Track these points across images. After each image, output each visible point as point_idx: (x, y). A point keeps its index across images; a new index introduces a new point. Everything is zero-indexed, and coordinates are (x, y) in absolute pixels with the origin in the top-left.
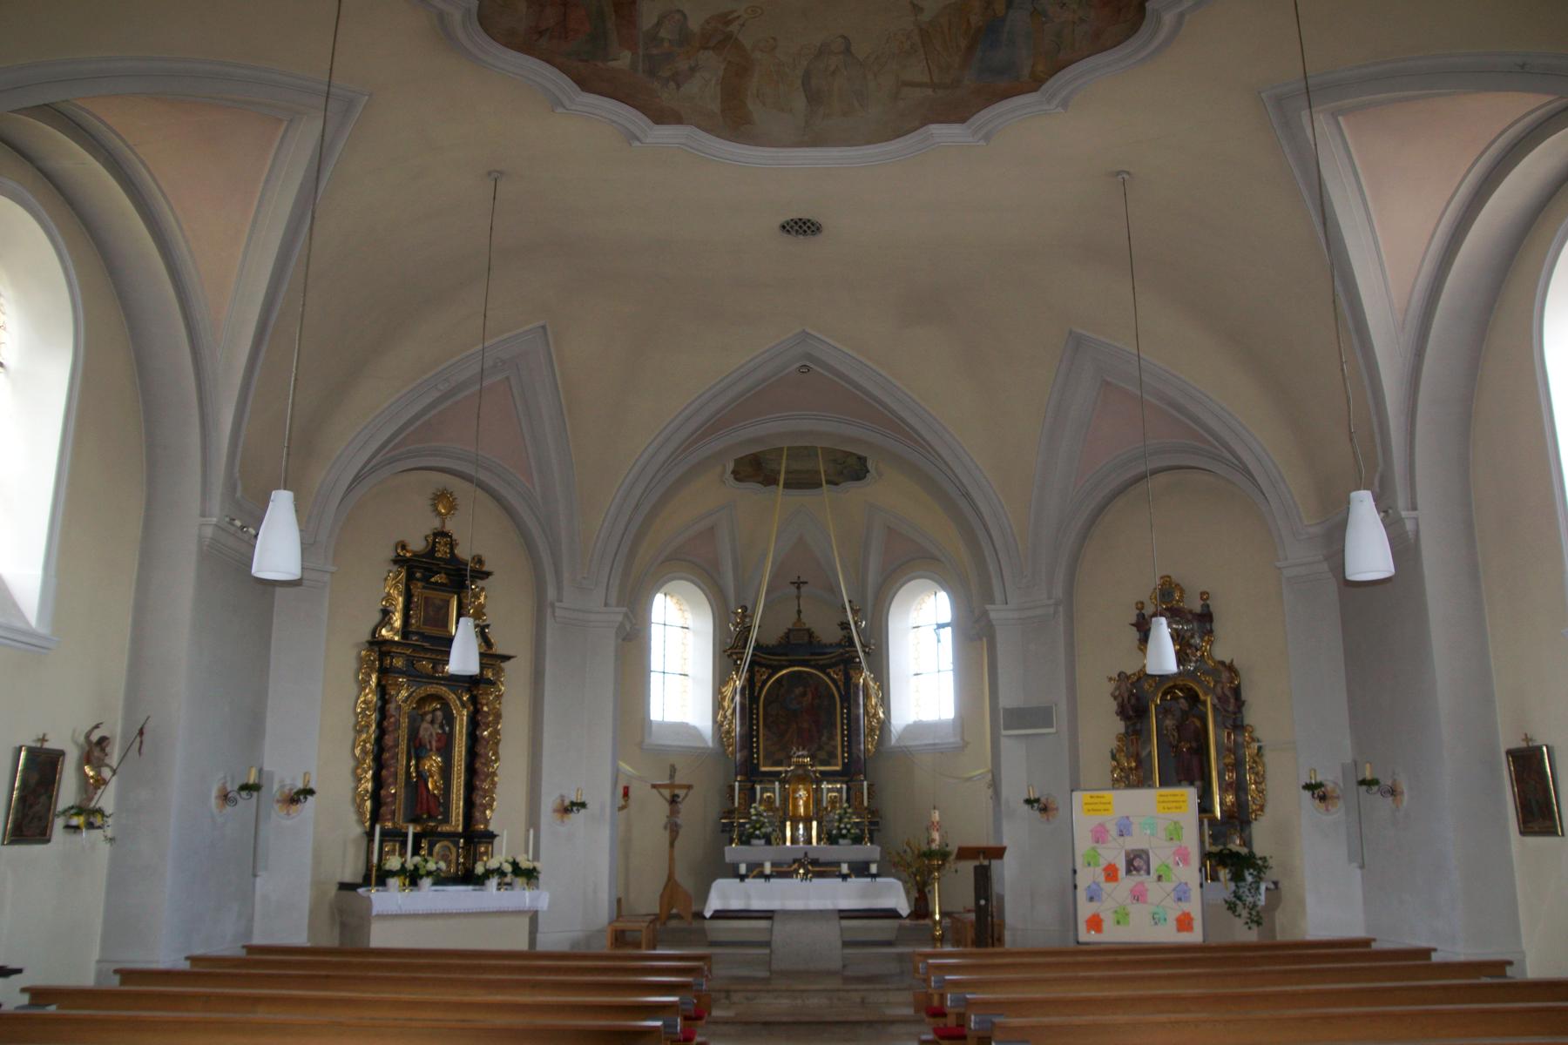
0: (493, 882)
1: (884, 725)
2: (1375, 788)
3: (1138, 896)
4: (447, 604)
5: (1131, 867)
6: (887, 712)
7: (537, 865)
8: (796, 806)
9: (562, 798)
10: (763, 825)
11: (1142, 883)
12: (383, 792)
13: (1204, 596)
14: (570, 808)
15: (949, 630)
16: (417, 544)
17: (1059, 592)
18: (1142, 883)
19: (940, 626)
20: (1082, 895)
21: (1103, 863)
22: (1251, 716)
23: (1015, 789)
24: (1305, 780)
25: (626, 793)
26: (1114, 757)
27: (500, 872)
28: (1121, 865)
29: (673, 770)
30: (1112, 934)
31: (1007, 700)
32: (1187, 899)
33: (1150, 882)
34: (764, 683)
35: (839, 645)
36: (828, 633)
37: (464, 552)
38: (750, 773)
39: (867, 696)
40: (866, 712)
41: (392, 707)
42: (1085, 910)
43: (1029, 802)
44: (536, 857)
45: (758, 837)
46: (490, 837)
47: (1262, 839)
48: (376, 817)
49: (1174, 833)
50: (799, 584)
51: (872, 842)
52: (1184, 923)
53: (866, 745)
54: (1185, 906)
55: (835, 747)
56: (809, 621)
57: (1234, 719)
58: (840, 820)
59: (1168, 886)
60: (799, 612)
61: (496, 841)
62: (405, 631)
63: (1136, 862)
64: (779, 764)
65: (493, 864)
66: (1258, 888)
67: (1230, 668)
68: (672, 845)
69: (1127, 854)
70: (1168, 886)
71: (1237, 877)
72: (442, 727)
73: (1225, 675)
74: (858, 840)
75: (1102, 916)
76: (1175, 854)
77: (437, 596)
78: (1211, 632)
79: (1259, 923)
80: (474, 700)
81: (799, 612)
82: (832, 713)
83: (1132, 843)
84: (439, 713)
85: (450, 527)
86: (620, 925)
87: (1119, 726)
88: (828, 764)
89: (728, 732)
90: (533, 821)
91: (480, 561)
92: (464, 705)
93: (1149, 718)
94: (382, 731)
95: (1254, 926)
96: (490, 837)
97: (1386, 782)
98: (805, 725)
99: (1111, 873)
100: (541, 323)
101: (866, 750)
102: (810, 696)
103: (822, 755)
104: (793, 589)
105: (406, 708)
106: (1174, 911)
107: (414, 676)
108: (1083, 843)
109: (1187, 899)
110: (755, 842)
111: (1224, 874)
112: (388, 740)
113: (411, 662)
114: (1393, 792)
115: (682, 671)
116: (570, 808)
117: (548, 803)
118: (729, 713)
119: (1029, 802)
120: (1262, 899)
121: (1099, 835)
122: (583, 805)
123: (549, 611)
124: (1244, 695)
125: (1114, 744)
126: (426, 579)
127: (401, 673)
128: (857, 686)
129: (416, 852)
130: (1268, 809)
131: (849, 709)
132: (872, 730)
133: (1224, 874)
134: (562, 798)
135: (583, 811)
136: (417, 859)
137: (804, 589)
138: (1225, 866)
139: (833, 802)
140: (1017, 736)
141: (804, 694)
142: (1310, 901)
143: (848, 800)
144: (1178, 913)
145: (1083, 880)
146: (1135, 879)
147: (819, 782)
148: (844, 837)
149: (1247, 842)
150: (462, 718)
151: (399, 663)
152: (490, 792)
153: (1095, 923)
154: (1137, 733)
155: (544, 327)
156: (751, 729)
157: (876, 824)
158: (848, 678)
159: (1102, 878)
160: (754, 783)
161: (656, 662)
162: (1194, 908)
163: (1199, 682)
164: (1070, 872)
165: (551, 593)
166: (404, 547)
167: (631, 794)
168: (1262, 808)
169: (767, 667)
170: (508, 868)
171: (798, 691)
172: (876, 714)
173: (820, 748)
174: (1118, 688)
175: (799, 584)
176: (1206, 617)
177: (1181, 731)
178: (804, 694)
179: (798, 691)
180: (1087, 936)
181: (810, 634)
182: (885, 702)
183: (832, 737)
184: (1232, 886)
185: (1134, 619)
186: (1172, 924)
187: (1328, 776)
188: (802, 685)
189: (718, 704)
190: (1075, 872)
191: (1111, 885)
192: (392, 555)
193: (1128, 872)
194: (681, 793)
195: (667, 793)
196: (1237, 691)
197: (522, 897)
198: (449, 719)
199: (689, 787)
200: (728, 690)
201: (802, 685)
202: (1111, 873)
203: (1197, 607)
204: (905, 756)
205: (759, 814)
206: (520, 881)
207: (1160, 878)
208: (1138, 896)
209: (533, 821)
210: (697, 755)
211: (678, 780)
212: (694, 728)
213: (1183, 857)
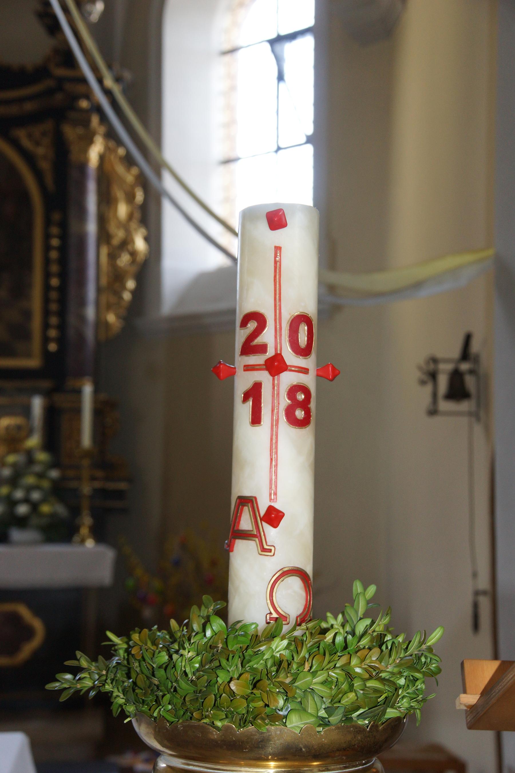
1: (148, 270)
6: (155, 240)
15: (308, 42)
35: (41, 72)
39: (106, 199)
40: (104, 235)
51: (100, 534)
55: (28, 315)
58: (14, 481)
74: (60, 531)
101: (101, 323)
128: (83, 166)
131: (64, 225)
132: (118, 277)
148: (22, 522)
157: (120, 495)
172: (126, 243)
182: (149, 216)
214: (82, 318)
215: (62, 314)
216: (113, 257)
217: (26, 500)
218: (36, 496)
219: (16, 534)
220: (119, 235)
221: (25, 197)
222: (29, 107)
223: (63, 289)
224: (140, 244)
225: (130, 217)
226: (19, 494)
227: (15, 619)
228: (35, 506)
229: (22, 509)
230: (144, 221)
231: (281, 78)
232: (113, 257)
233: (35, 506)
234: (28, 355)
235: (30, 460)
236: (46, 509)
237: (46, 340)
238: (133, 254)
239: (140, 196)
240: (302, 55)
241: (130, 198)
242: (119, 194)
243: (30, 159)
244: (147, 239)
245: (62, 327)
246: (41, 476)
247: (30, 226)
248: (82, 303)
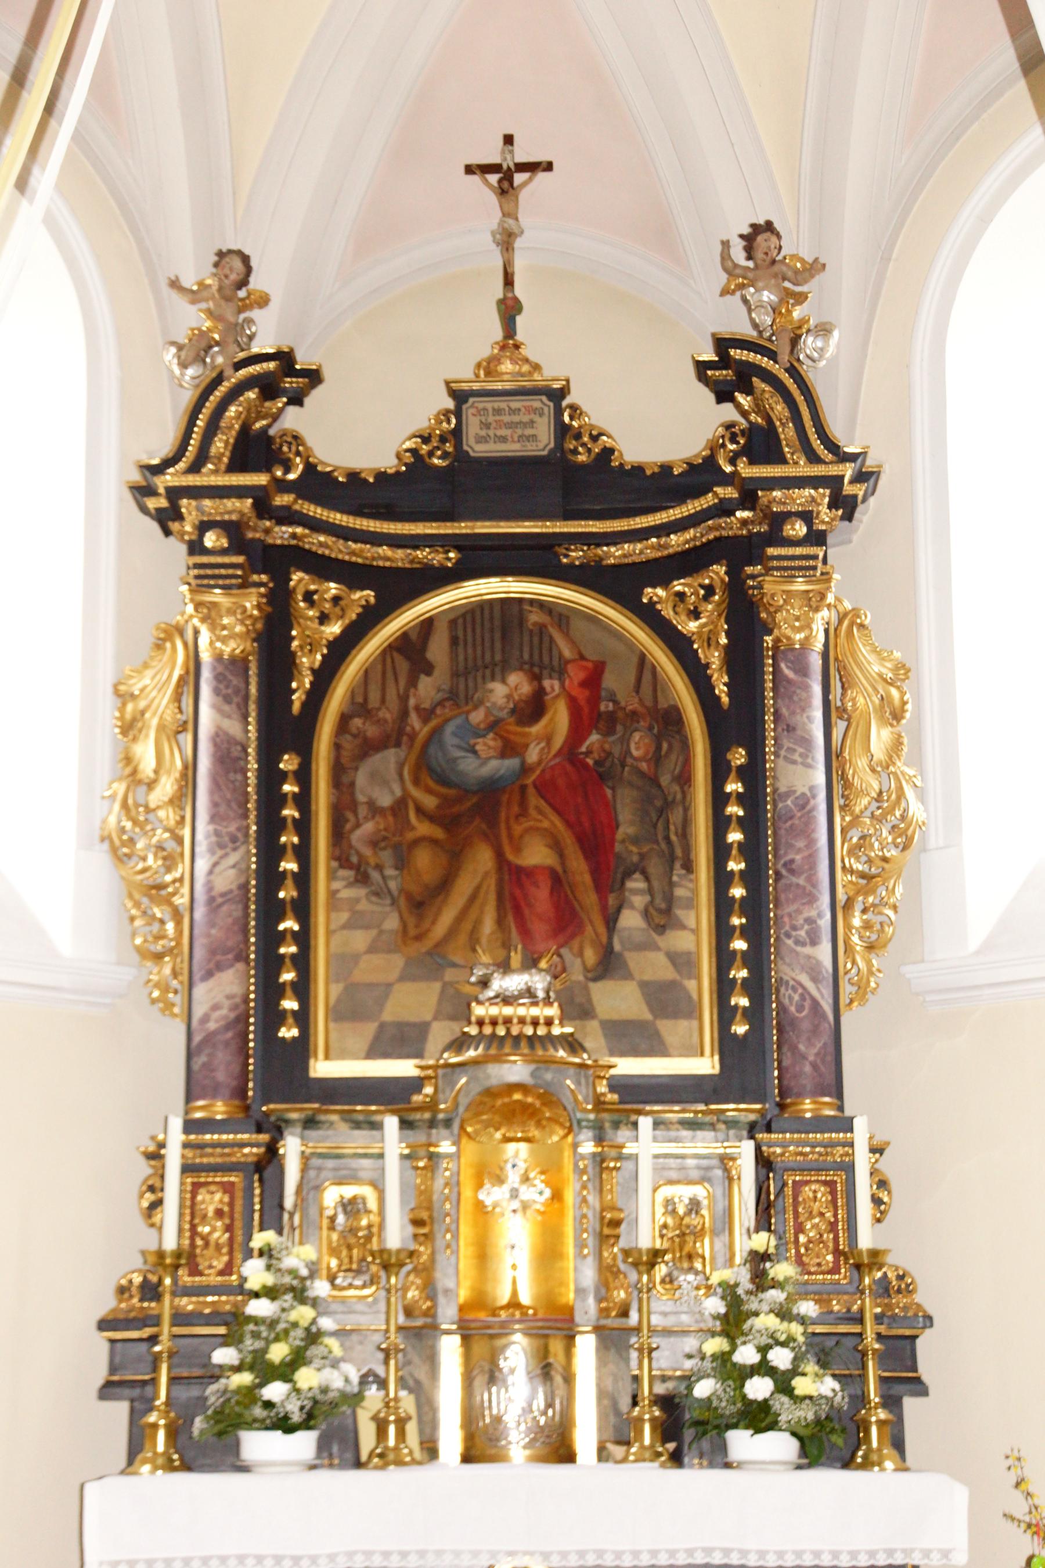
8: (483, 1256)
34: (340, 651)
35: (702, 474)
36: (655, 414)
38: (260, 1081)
45: (285, 1425)
50: (506, 176)
55: (685, 963)
56: (551, 346)
58: (733, 1322)
60: (509, 310)
82: (663, 806)
88: (657, 1048)
98: (536, 855)
102: (559, 719)
103: (617, 999)
104: (481, 192)
110: (258, 1444)
131: (754, 775)
139: (682, 1242)
141: (534, 708)
143: (765, 1213)
148: (759, 1418)
156: (269, 877)
158: (746, 620)
160: (275, 1130)
169: (353, 575)
171: (505, 690)
173: (609, 965)
175: (506, 176)
178: (534, 708)
179: (505, 690)
215: (757, 959)
217: (764, 1368)
218: (781, 1358)
221: (671, 721)
222: (676, 541)
223: (755, 907)
226: (746, 1355)
229: (759, 1388)
233: (784, 1383)
236: (802, 1385)
237: (725, 1014)
243: (679, 646)
245: (757, 987)
246: (784, 1314)
247: (685, 779)
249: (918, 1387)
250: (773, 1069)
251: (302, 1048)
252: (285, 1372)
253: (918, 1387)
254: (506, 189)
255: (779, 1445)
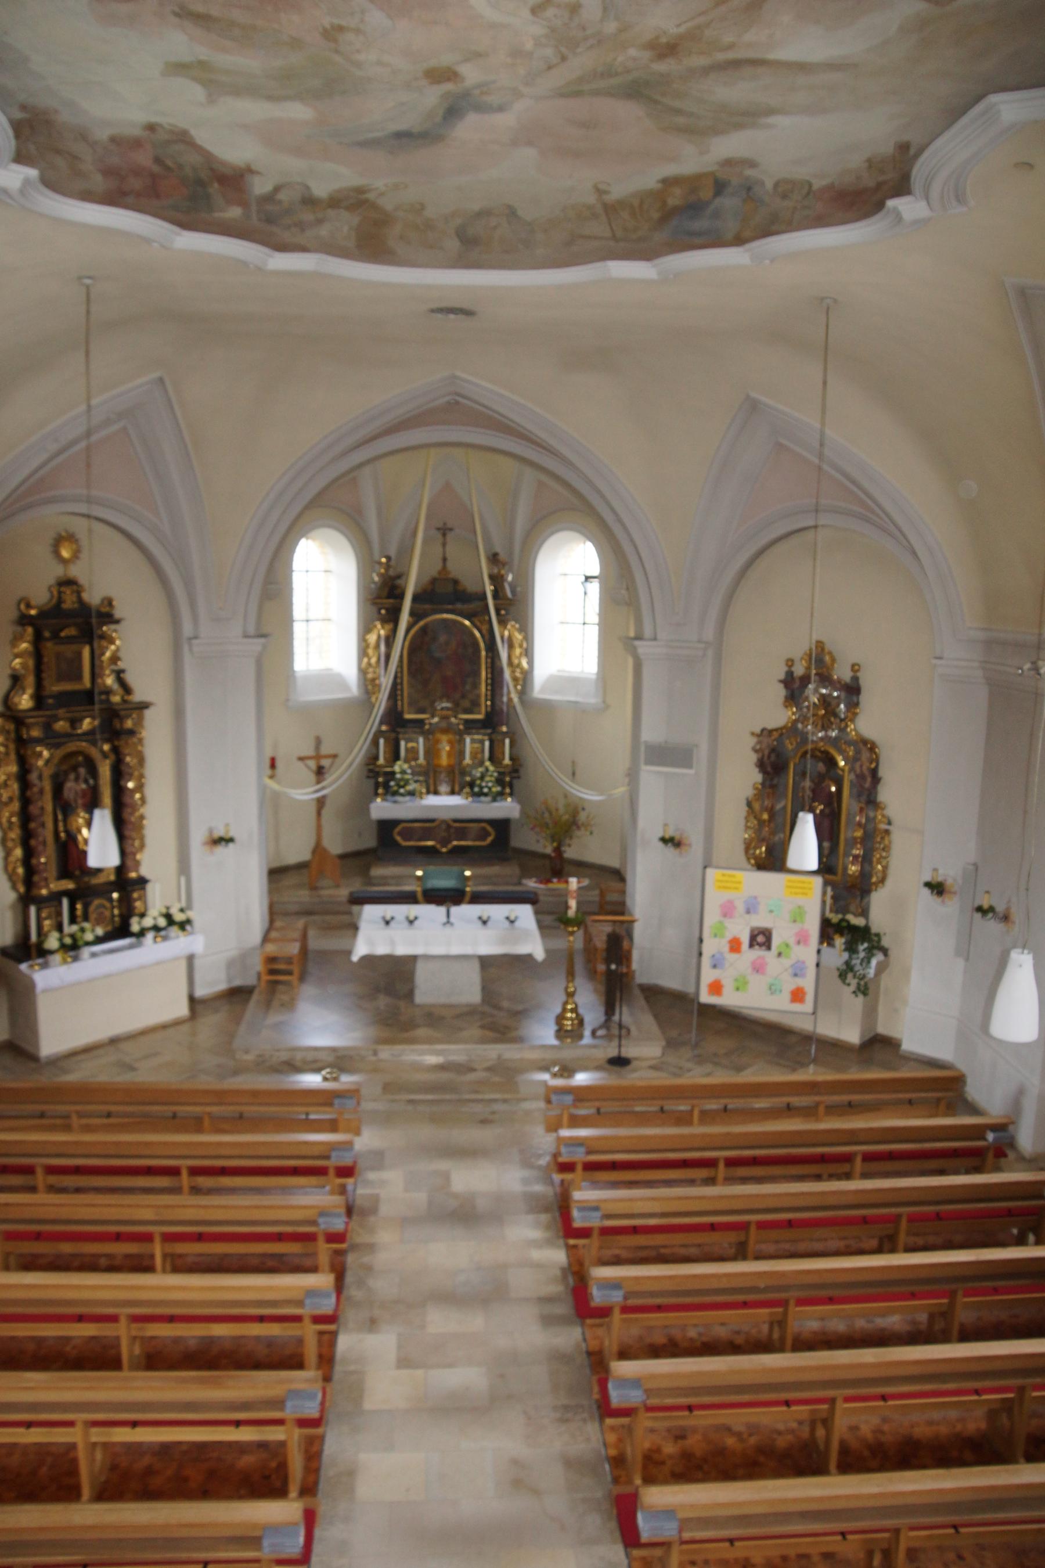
0: (150, 936)
2: (990, 915)
3: (758, 968)
4: (79, 655)
5: (753, 942)
6: (531, 663)
7: (190, 914)
9: (211, 831)
10: (407, 782)
11: (763, 958)
12: (34, 861)
13: (855, 668)
14: (220, 841)
16: (41, 597)
17: (709, 634)
18: (763, 958)
19: (587, 578)
20: (706, 961)
21: (729, 936)
22: (885, 794)
23: (651, 821)
24: (928, 878)
25: (273, 764)
26: (749, 804)
27: (156, 928)
28: (745, 940)
29: (318, 742)
30: (729, 999)
31: (652, 733)
32: (803, 976)
33: (770, 956)
37: (93, 597)
39: (511, 646)
41: (33, 777)
42: (708, 975)
43: (664, 840)
44: (189, 906)
46: (142, 882)
47: (879, 911)
48: (29, 881)
49: (798, 916)
52: (797, 995)
53: (511, 692)
54: (800, 982)
55: (479, 696)
57: (870, 799)
58: (482, 778)
59: (786, 962)
60: (445, 560)
61: (149, 887)
62: (39, 698)
63: (761, 938)
64: (422, 711)
65: (148, 922)
66: (869, 962)
67: (871, 746)
68: (319, 813)
69: (752, 930)
70: (786, 962)
71: (851, 948)
72: (86, 781)
73: (865, 755)
74: (497, 797)
75: (724, 982)
76: (797, 934)
77: (68, 650)
78: (857, 704)
79: (865, 993)
80: (115, 750)
81: (445, 560)
83: (761, 921)
84: (82, 771)
85: (75, 571)
86: (271, 949)
87: (758, 777)
89: (373, 680)
90: (184, 867)
91: (109, 602)
92: (105, 755)
93: (787, 774)
94: (26, 801)
95: (861, 997)
96: (142, 882)
97: (1000, 908)
99: (735, 946)
100: (155, 375)
103: (466, 703)
105: (47, 773)
106: (790, 984)
107: (52, 739)
108: (712, 917)
109: (803, 976)
111: (839, 941)
112: (33, 809)
113: (47, 727)
114: (1006, 918)
115: (326, 620)
116: (220, 841)
117: (198, 836)
118: (373, 660)
119: (664, 840)
120: (871, 972)
121: (728, 910)
122: (231, 840)
123: (186, 648)
124: (882, 772)
125: (750, 792)
126: (55, 636)
127: (38, 741)
129: (73, 920)
130: (889, 882)
133: (839, 941)
134: (211, 831)
135: (231, 845)
136: (75, 928)
137: (450, 536)
138: (842, 935)
140: (659, 773)
142: (914, 976)
144: (793, 987)
145: (709, 947)
146: (758, 953)
147: (461, 734)
148: (486, 795)
149: (865, 913)
150: (105, 770)
151: (35, 733)
152: (139, 827)
153: (716, 988)
154: (773, 787)
155: (161, 380)
159: (726, 948)
161: (298, 611)
162: (808, 983)
163: (841, 752)
164: (696, 940)
165: (187, 629)
166: (29, 606)
167: (279, 764)
168: (883, 880)
170: (162, 922)
172: (519, 665)
173: (463, 696)
174: (759, 742)
176: (853, 690)
177: (814, 774)
180: (706, 998)
181: (456, 582)
182: (528, 653)
183: (476, 685)
184: (846, 956)
185: (782, 676)
186: (786, 996)
187: (950, 873)
188: (445, 634)
189: (363, 651)
190: (701, 941)
191: (734, 956)
192: (14, 614)
193: (751, 946)
194: (325, 763)
195: (312, 764)
196: (874, 772)
197: (179, 944)
198: (93, 771)
199: (335, 756)
200: (372, 638)
201: (445, 634)
202: (735, 946)
203: (846, 676)
204: (547, 708)
205: (403, 772)
206: (174, 931)
207: (780, 954)
208: (758, 968)
209: (184, 867)
210: (343, 707)
211: (325, 750)
212: (339, 675)
213: (802, 939)
214: (502, 702)
216: (513, 672)
218: (490, 784)
219: (483, 798)
220: (516, 661)
224: (524, 663)
225: (521, 654)
226: (484, 784)
227: (484, 829)
228: (490, 788)
229: (486, 790)
230: (526, 655)
231: (585, 593)
232: (513, 672)
234: (479, 713)
235: (487, 770)
238: (522, 669)
239: (525, 645)
240: (594, 587)
241: (521, 646)
242: (517, 645)
244: (528, 663)
248: (502, 695)
249: (519, 777)
250: (493, 722)
251: (401, 713)
252: (403, 787)
253: (519, 777)
254: (444, 535)
255: (488, 799)
